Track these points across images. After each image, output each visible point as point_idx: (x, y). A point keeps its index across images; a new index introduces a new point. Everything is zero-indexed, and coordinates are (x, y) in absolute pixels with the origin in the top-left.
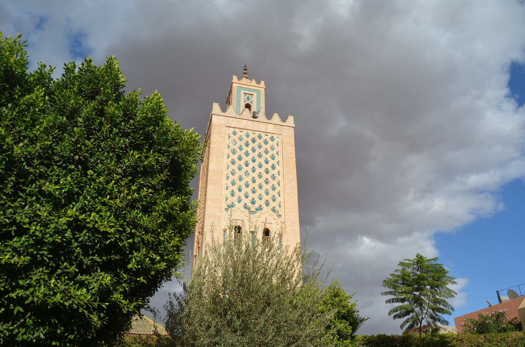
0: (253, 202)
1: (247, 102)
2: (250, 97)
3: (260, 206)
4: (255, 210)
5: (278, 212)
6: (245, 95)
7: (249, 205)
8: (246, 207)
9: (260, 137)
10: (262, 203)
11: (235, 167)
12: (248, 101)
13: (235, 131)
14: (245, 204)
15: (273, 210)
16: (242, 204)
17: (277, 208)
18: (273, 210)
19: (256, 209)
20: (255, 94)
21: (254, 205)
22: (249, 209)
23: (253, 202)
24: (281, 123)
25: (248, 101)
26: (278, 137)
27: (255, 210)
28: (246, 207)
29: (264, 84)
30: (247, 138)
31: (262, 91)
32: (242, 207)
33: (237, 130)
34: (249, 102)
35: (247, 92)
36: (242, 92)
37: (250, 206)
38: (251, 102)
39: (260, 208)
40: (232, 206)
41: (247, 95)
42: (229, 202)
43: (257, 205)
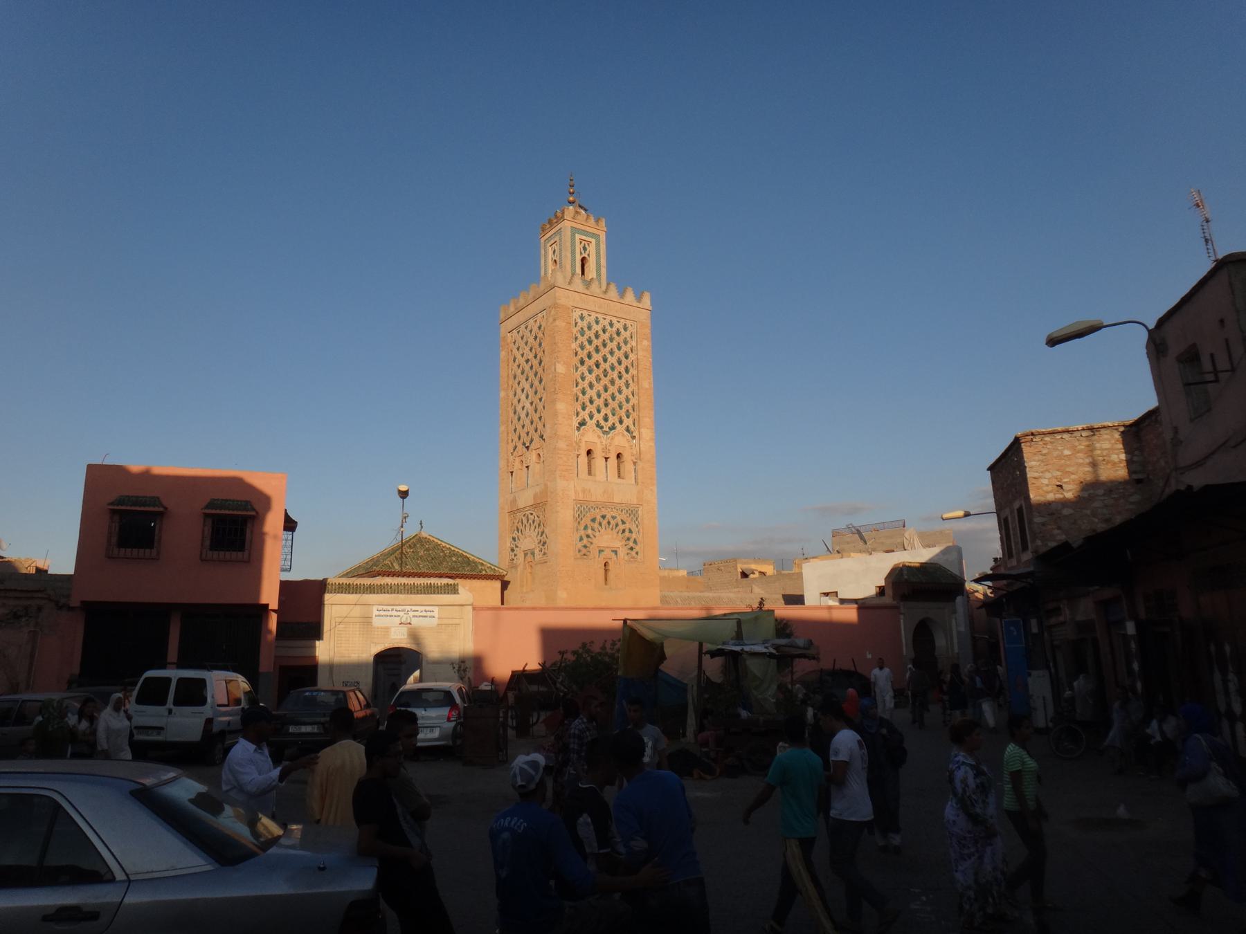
0: (606, 419)
1: (584, 255)
2: (587, 246)
3: (614, 424)
4: (608, 430)
5: (632, 433)
6: (581, 243)
7: (602, 423)
8: (598, 425)
11: (584, 369)
13: (582, 314)
14: (598, 421)
15: (628, 430)
16: (594, 421)
17: (632, 428)
18: (628, 430)
19: (609, 428)
20: (593, 241)
22: (602, 428)
23: (606, 419)
24: (635, 304)
26: (631, 325)
27: (608, 430)
28: (598, 425)
29: (604, 225)
32: (595, 426)
33: (585, 313)
35: (584, 238)
36: (578, 236)
37: (602, 424)
38: (589, 255)
39: (613, 428)
40: (583, 423)
41: (583, 242)
42: (580, 419)
43: (609, 424)
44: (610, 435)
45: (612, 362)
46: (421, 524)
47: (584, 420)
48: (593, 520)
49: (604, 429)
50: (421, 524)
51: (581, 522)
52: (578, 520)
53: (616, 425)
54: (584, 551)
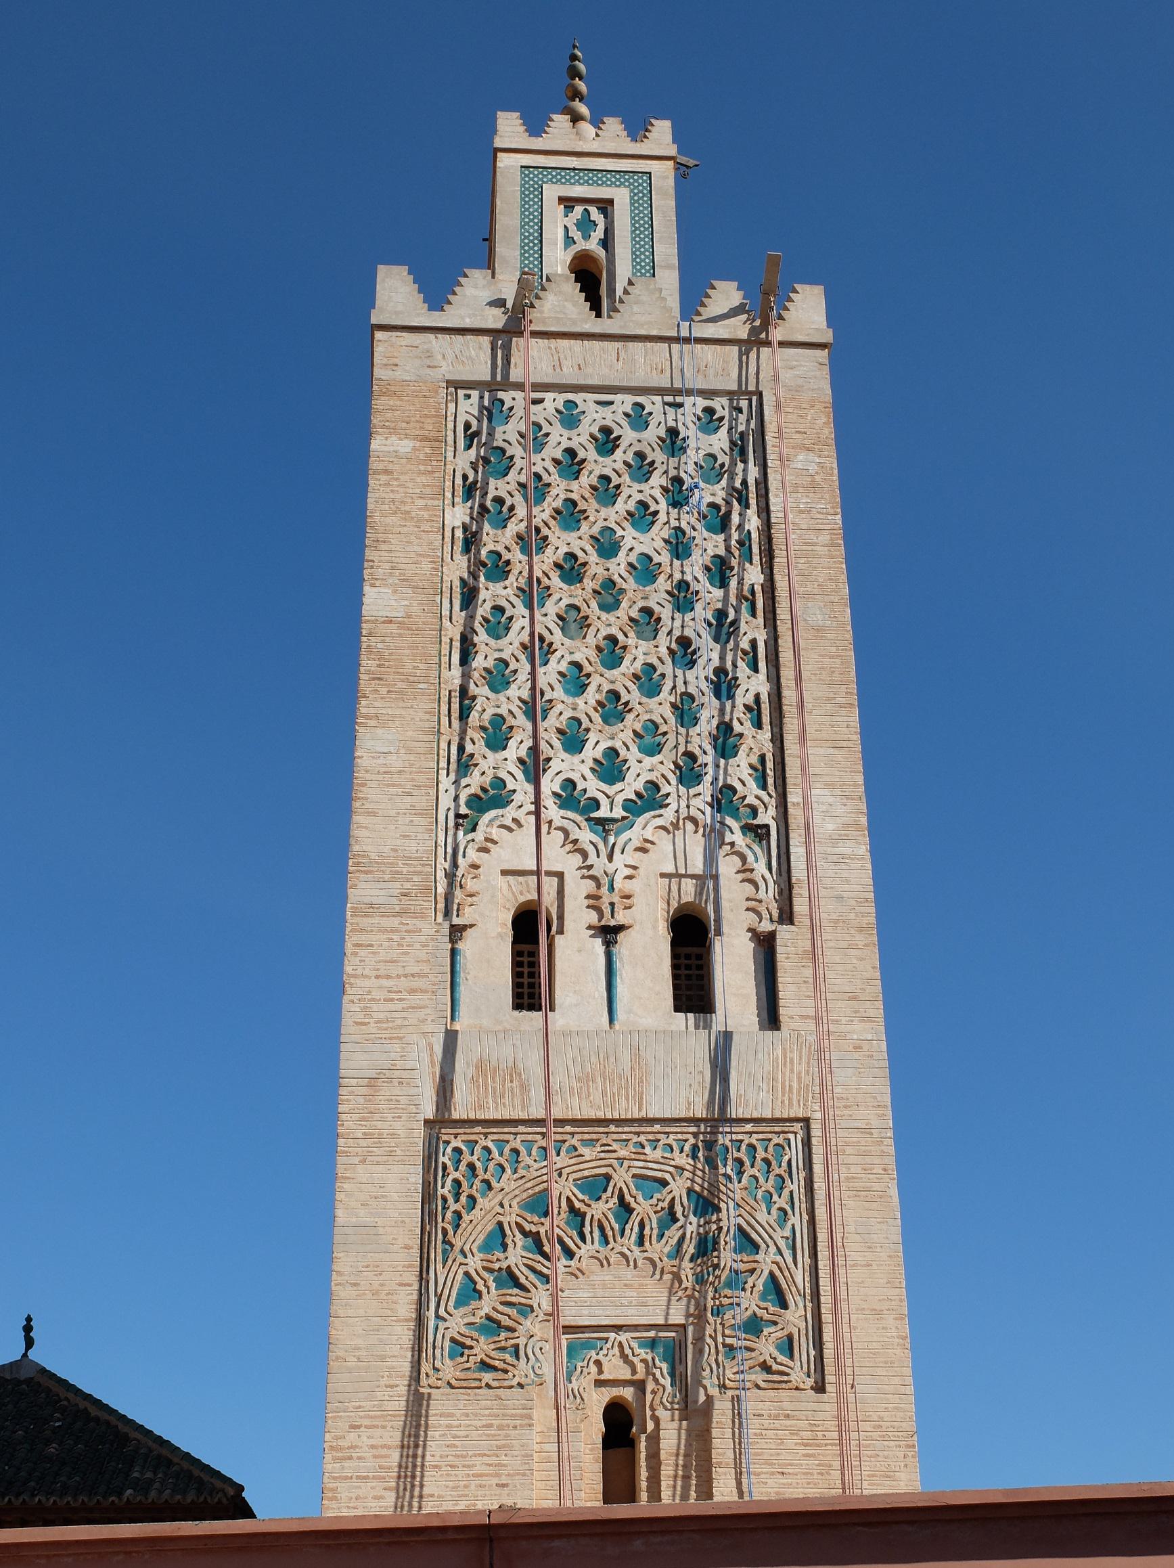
4: (618, 812)
7: (593, 786)
8: (569, 796)
9: (638, 418)
10: (661, 766)
12: (587, 237)
21: (619, 786)
25: (587, 237)
27: (618, 812)
28: (569, 796)
30: (566, 433)
31: (663, 174)
34: (593, 245)
36: (551, 193)
42: (475, 782)
43: (632, 785)
44: (635, 834)
45: (640, 549)
46: (28, 1329)
47: (500, 783)
48: (539, 1204)
49: (603, 812)
50: (28, 1329)
51: (466, 1218)
52: (453, 1206)
53: (665, 789)
54: (483, 1347)
